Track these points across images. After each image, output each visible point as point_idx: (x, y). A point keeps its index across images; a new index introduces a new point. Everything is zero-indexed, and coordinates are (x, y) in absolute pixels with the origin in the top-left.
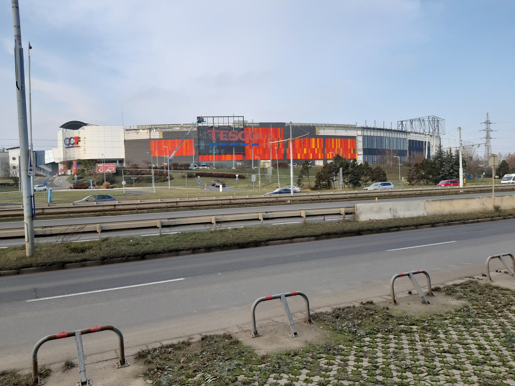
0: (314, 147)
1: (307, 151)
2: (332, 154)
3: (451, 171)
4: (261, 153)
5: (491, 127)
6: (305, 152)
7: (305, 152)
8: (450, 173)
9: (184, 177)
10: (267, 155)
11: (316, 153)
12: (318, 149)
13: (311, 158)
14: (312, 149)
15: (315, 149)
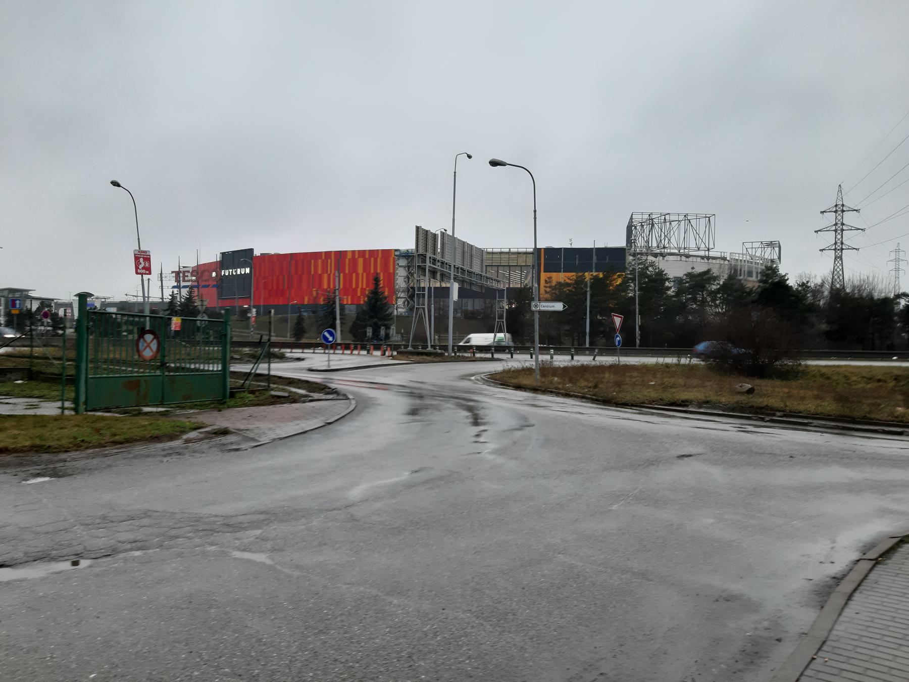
1: (317, 294)
6: (314, 294)
7: (314, 294)
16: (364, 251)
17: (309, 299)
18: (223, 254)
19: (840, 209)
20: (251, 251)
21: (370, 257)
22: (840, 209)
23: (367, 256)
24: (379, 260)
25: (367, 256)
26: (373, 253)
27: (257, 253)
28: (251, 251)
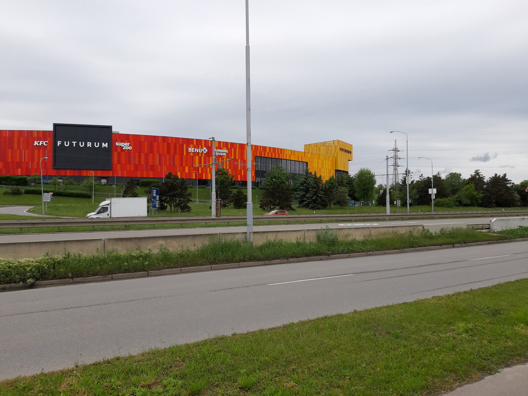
0: (197, 165)
1: (189, 170)
2: (196, 173)
3: (314, 198)
4: (132, 169)
5: (399, 154)
6: (187, 171)
7: (187, 171)
8: (313, 200)
9: (5, 193)
10: (139, 172)
11: (200, 172)
12: (202, 169)
13: (194, 178)
14: (195, 167)
15: (198, 168)
16: (227, 143)
17: (181, 175)
18: (56, 126)
19: (396, 150)
20: (110, 128)
21: (231, 148)
22: (396, 150)
23: (229, 147)
24: (237, 150)
25: (229, 147)
26: (233, 144)
27: (114, 130)
28: (110, 128)
